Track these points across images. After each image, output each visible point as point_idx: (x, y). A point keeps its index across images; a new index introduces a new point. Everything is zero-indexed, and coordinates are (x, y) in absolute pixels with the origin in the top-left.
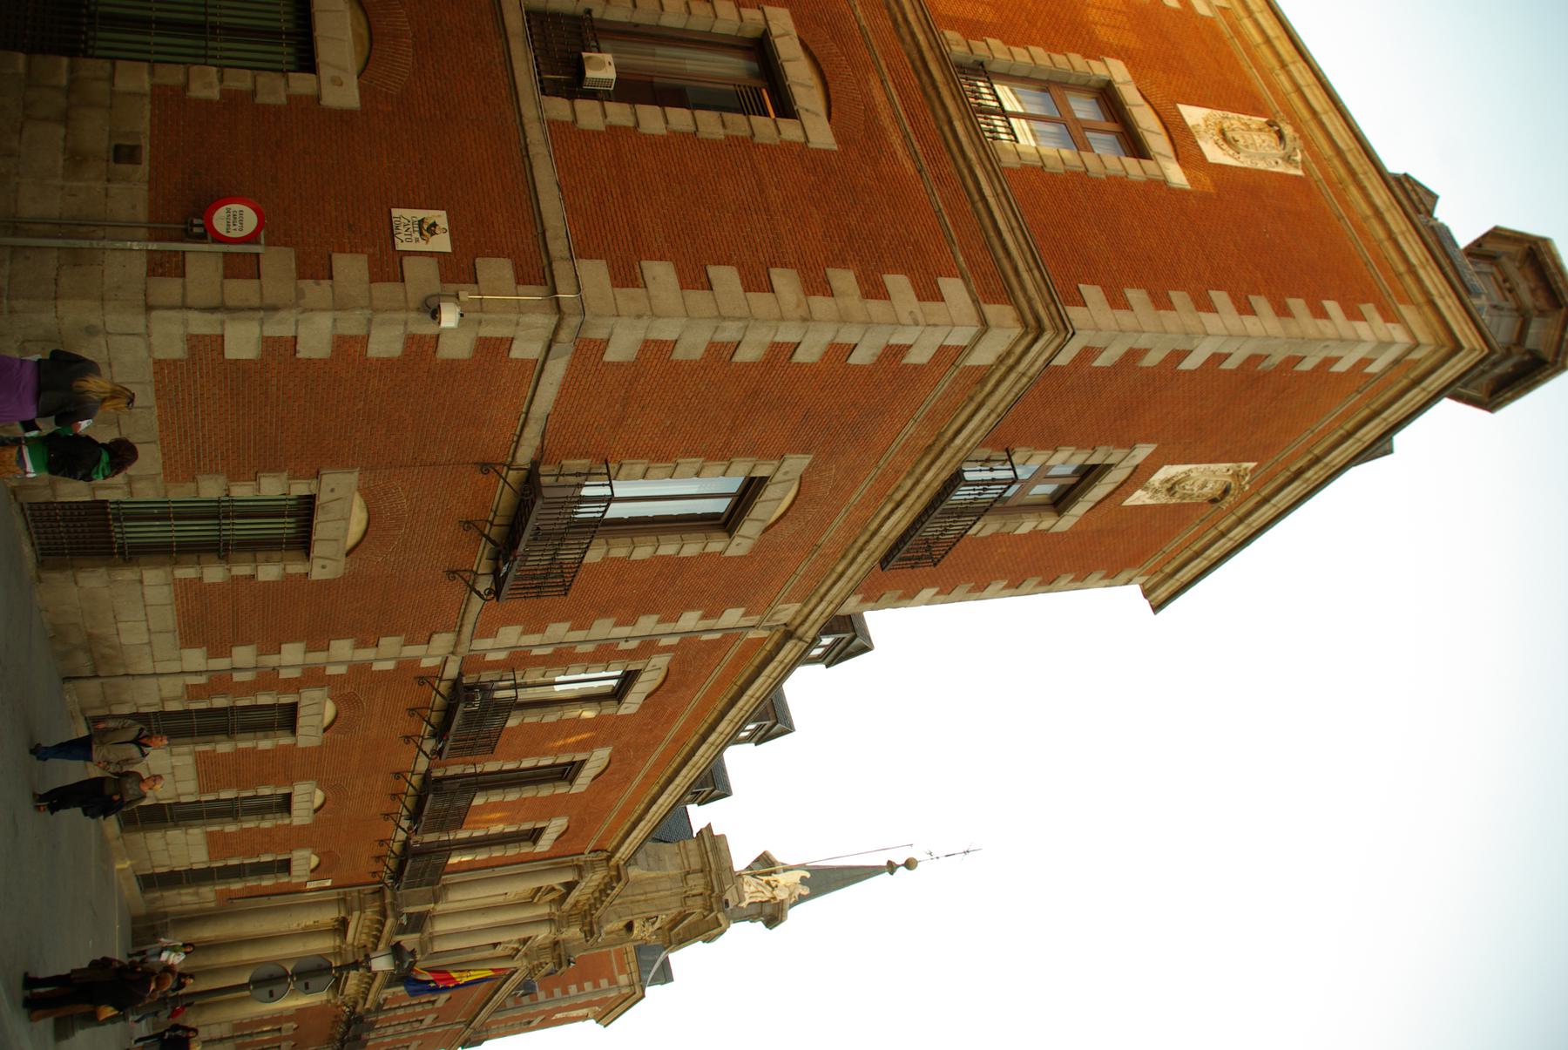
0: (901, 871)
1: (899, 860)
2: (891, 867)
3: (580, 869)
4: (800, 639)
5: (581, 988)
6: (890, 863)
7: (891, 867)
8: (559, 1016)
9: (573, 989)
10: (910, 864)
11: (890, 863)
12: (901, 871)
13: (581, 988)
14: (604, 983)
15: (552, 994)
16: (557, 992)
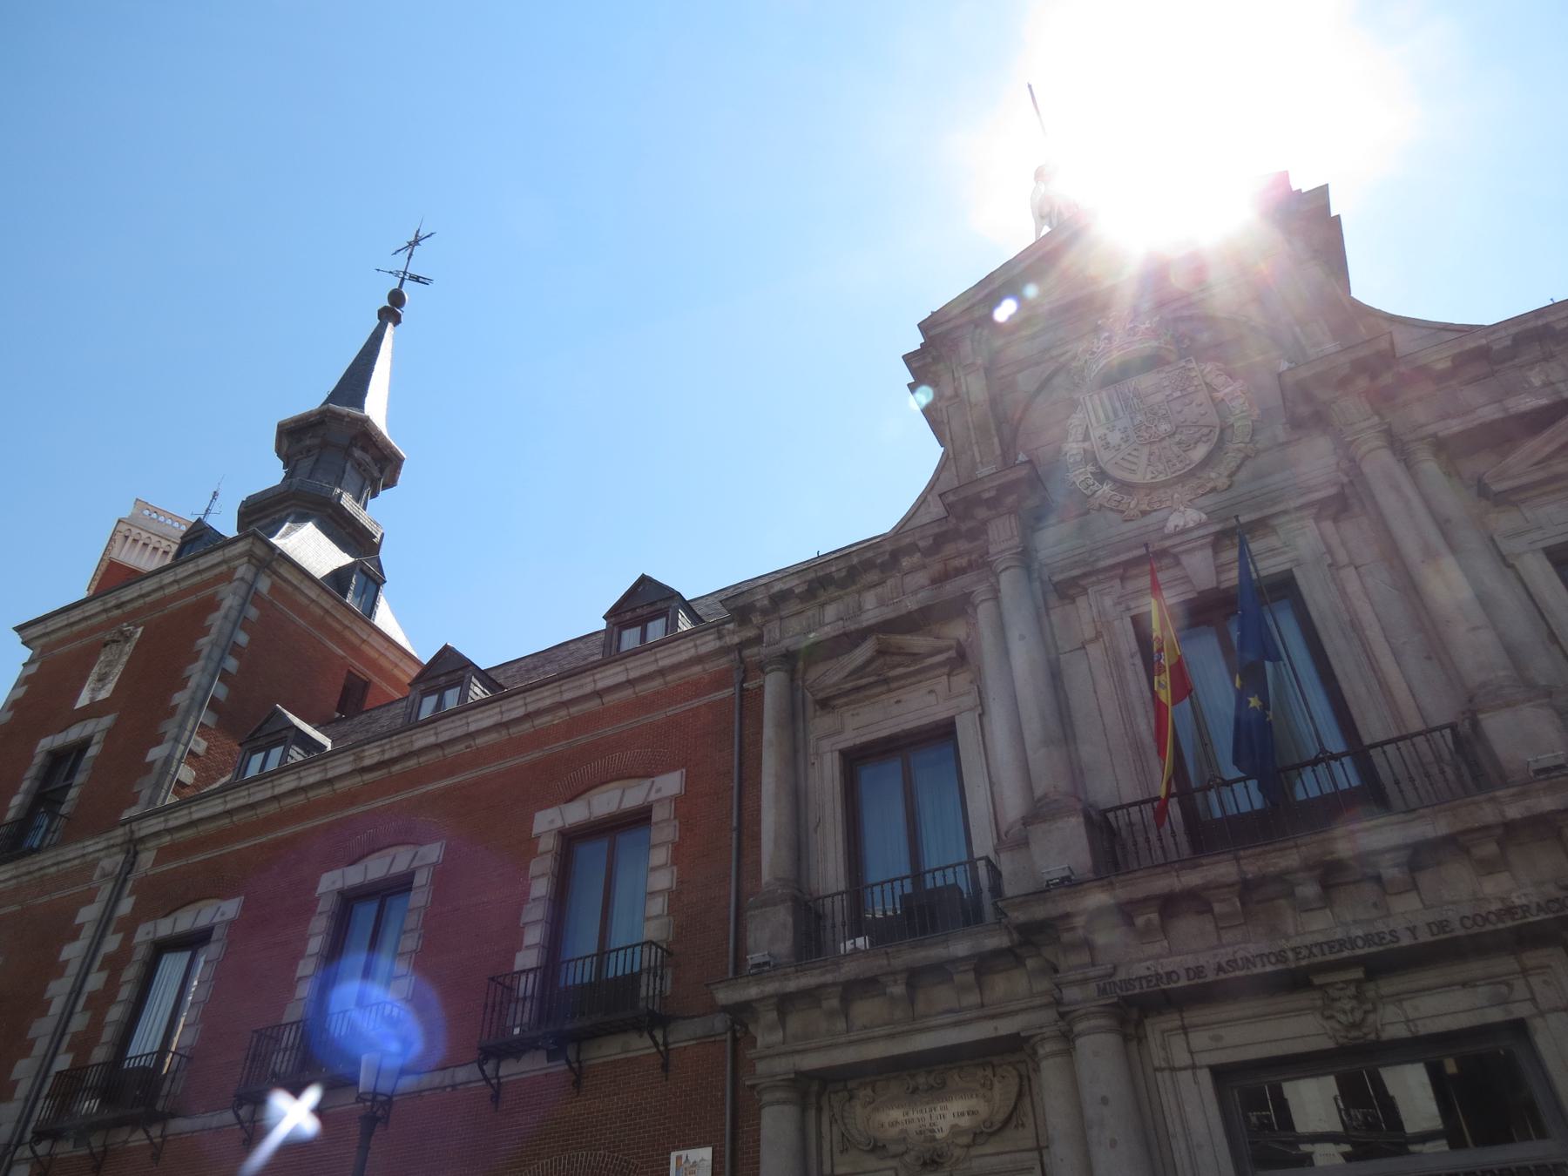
4: (132, 832)
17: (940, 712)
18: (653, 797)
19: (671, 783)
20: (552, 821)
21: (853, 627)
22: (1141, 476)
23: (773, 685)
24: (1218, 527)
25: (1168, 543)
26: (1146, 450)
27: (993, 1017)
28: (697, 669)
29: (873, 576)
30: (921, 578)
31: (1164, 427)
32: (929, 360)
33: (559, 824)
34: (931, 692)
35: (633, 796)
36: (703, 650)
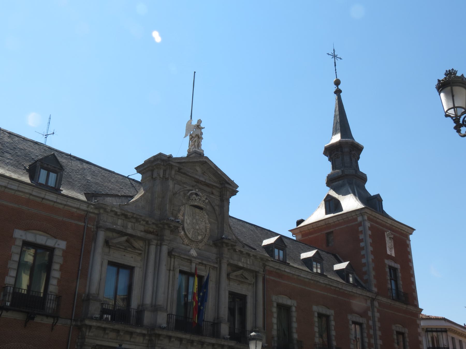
0: (340, 87)
1: (334, 88)
2: (338, 92)
3: (98, 228)
5: (362, 241)
6: (335, 93)
7: (338, 92)
8: (391, 252)
9: (362, 244)
10: (337, 83)
11: (335, 93)
12: (340, 87)
13: (362, 241)
14: (361, 229)
15: (364, 255)
16: (363, 252)
17: (132, 264)
18: (56, 246)
19: (62, 245)
20: (21, 236)
21: (124, 231)
22: (190, 236)
23: (101, 236)
24: (200, 261)
25: (193, 259)
26: (192, 230)
27: (136, 345)
28: (75, 210)
29: (134, 220)
30: (142, 228)
31: (197, 227)
32: (162, 164)
33: (24, 238)
34: (132, 257)
35: (51, 243)
36: (82, 207)
